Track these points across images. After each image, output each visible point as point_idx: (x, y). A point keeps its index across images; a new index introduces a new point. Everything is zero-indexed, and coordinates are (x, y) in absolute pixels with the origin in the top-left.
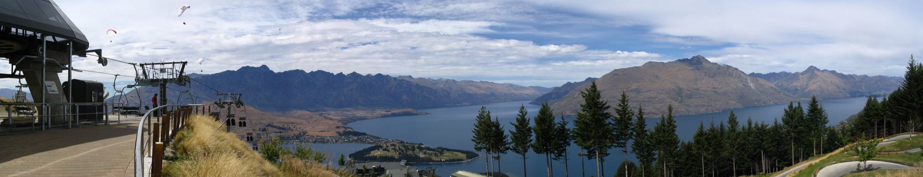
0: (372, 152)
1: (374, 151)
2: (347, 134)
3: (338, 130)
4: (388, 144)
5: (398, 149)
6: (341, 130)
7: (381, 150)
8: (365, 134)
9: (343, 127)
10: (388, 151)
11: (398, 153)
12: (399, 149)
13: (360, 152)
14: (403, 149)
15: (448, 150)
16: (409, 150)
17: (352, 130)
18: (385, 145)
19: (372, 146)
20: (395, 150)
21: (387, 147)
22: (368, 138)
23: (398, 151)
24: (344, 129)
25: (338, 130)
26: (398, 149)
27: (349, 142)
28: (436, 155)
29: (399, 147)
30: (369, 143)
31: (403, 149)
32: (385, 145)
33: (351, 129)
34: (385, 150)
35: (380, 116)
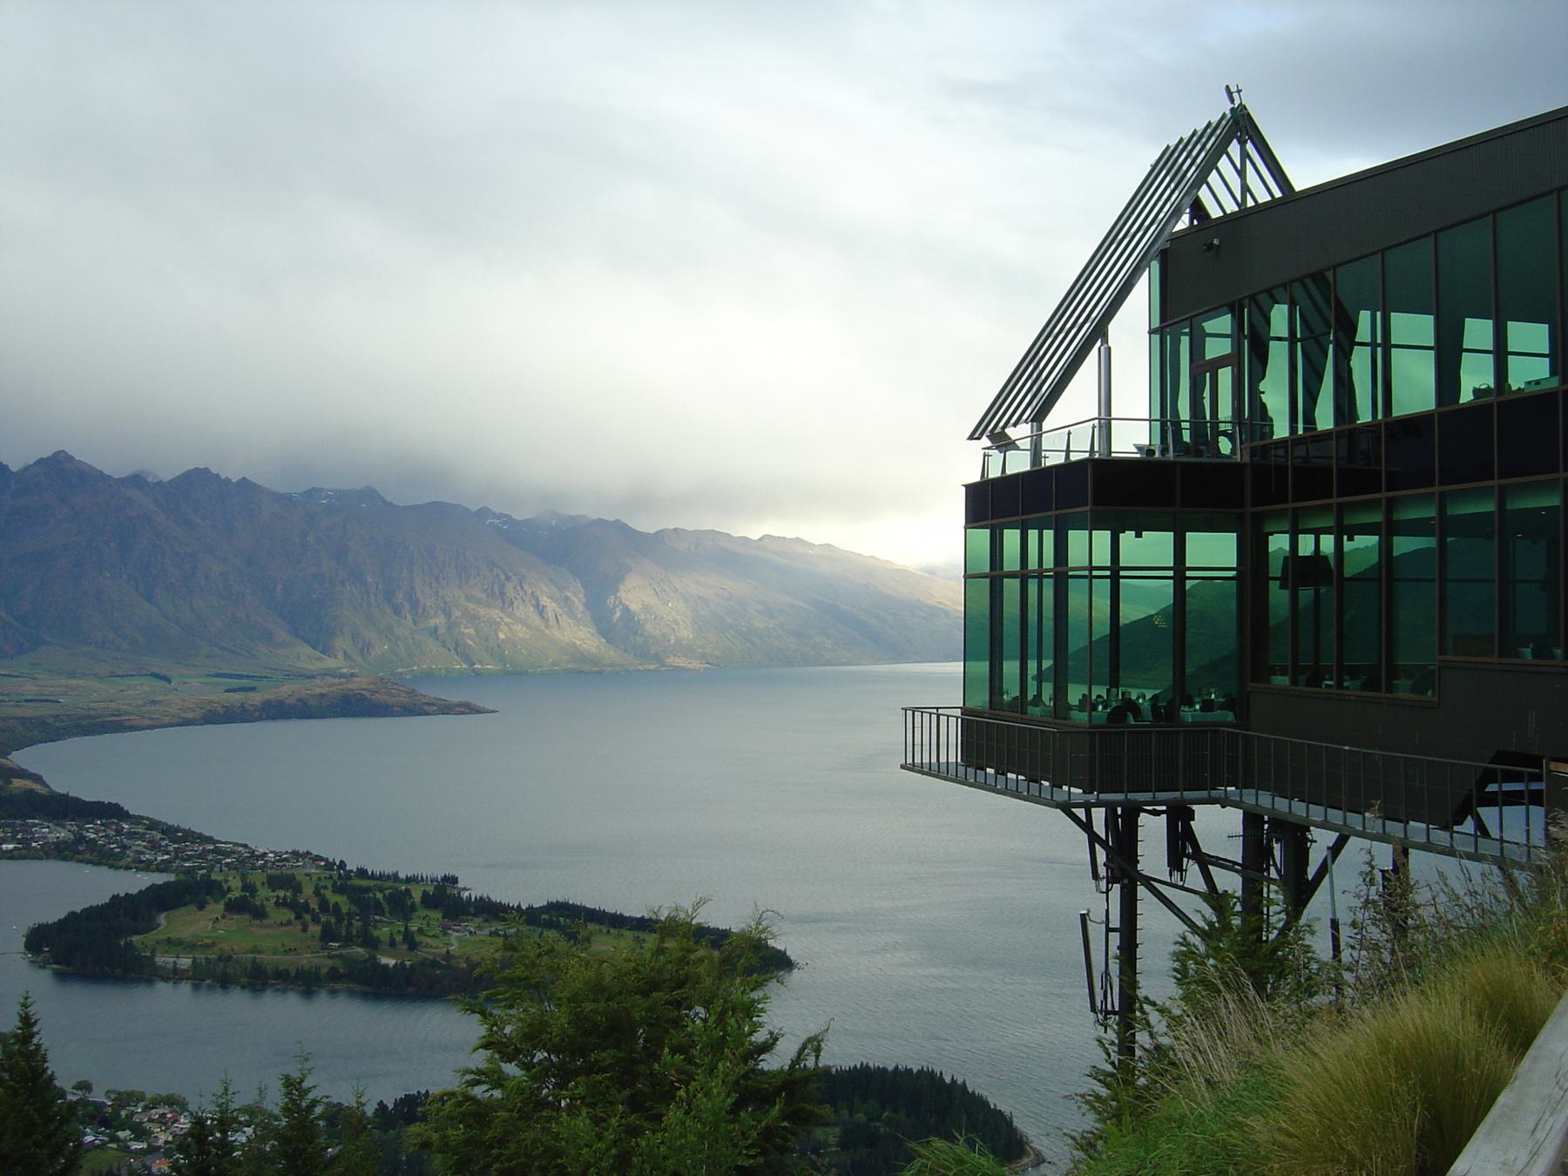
0: (162, 919)
1: (180, 914)
4: (257, 878)
5: (314, 905)
7: (217, 908)
8: (113, 812)
10: (259, 914)
11: (315, 929)
12: (324, 905)
13: (91, 913)
14: (344, 903)
15: (616, 921)
16: (381, 912)
17: (37, 787)
18: (235, 883)
19: (159, 879)
20: (300, 910)
21: (248, 887)
22: (132, 835)
23: (316, 920)
26: (314, 905)
27: (25, 853)
29: (317, 892)
30: (147, 867)
31: (344, 903)
32: (235, 883)
33: (37, 778)
34: (234, 907)
35: (198, 714)
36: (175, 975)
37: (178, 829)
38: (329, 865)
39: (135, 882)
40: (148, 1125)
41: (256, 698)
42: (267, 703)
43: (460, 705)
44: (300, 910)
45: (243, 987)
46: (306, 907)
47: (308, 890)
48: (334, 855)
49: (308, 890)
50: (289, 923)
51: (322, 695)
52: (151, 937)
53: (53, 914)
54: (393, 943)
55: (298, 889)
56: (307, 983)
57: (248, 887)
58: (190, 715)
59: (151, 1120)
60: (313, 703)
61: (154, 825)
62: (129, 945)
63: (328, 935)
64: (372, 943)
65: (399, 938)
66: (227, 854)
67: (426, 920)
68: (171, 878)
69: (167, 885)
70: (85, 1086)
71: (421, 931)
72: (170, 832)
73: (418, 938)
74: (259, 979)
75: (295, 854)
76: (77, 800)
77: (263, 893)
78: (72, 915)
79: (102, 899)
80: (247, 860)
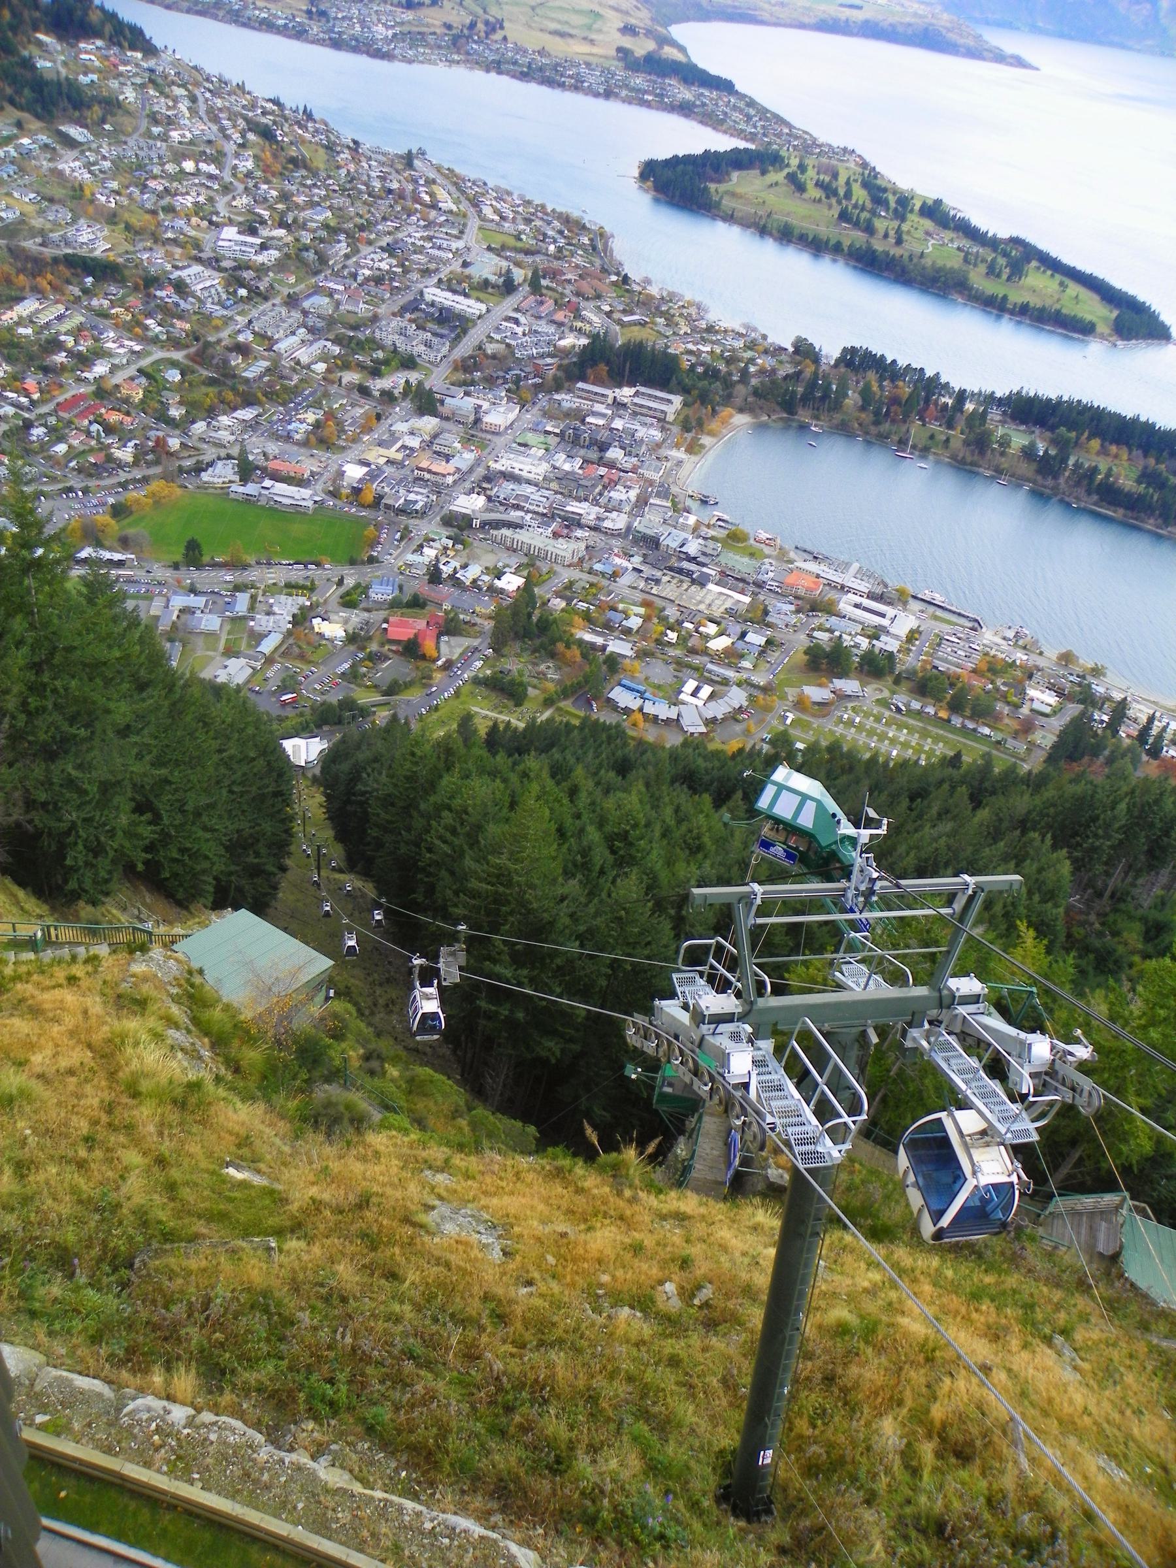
0: (735, 175)
2: (655, 65)
3: (627, 42)
6: (642, 47)
8: (725, 86)
9: (649, 33)
13: (689, 159)
19: (742, 145)
20: (829, 190)
21: (802, 168)
22: (735, 108)
23: (839, 202)
24: (651, 46)
25: (627, 42)
28: (992, 271)
29: (848, 183)
30: (740, 134)
32: (794, 162)
33: (682, 49)
35: (813, 21)
36: (730, 218)
37: (767, 111)
38: (865, 165)
39: (723, 143)
40: (677, 319)
41: (858, 16)
42: (866, 22)
43: (1012, 56)
44: (829, 190)
45: (775, 239)
46: (835, 193)
47: (842, 180)
48: (873, 161)
49: (842, 180)
50: (820, 201)
51: (909, 25)
52: (722, 187)
53: (663, 154)
54: (886, 236)
55: (835, 176)
56: (816, 246)
57: (802, 168)
58: (806, 20)
59: (681, 315)
60: (900, 29)
61: (752, 103)
62: (706, 189)
63: (844, 216)
64: (869, 229)
65: (892, 233)
66: (797, 138)
67: (916, 224)
68: (752, 147)
69: (746, 150)
70: (648, 281)
71: (909, 232)
72: (763, 112)
73: (905, 237)
74: (786, 235)
75: (845, 150)
76: (704, 72)
77: (811, 173)
78: (676, 157)
79: (698, 150)
80: (809, 146)
